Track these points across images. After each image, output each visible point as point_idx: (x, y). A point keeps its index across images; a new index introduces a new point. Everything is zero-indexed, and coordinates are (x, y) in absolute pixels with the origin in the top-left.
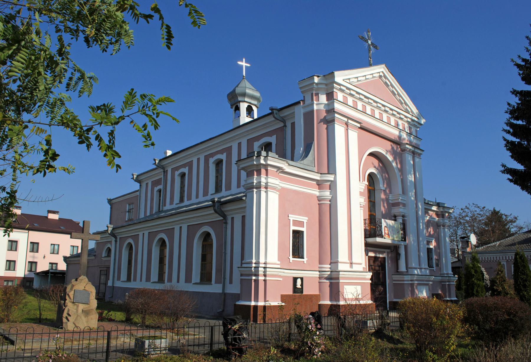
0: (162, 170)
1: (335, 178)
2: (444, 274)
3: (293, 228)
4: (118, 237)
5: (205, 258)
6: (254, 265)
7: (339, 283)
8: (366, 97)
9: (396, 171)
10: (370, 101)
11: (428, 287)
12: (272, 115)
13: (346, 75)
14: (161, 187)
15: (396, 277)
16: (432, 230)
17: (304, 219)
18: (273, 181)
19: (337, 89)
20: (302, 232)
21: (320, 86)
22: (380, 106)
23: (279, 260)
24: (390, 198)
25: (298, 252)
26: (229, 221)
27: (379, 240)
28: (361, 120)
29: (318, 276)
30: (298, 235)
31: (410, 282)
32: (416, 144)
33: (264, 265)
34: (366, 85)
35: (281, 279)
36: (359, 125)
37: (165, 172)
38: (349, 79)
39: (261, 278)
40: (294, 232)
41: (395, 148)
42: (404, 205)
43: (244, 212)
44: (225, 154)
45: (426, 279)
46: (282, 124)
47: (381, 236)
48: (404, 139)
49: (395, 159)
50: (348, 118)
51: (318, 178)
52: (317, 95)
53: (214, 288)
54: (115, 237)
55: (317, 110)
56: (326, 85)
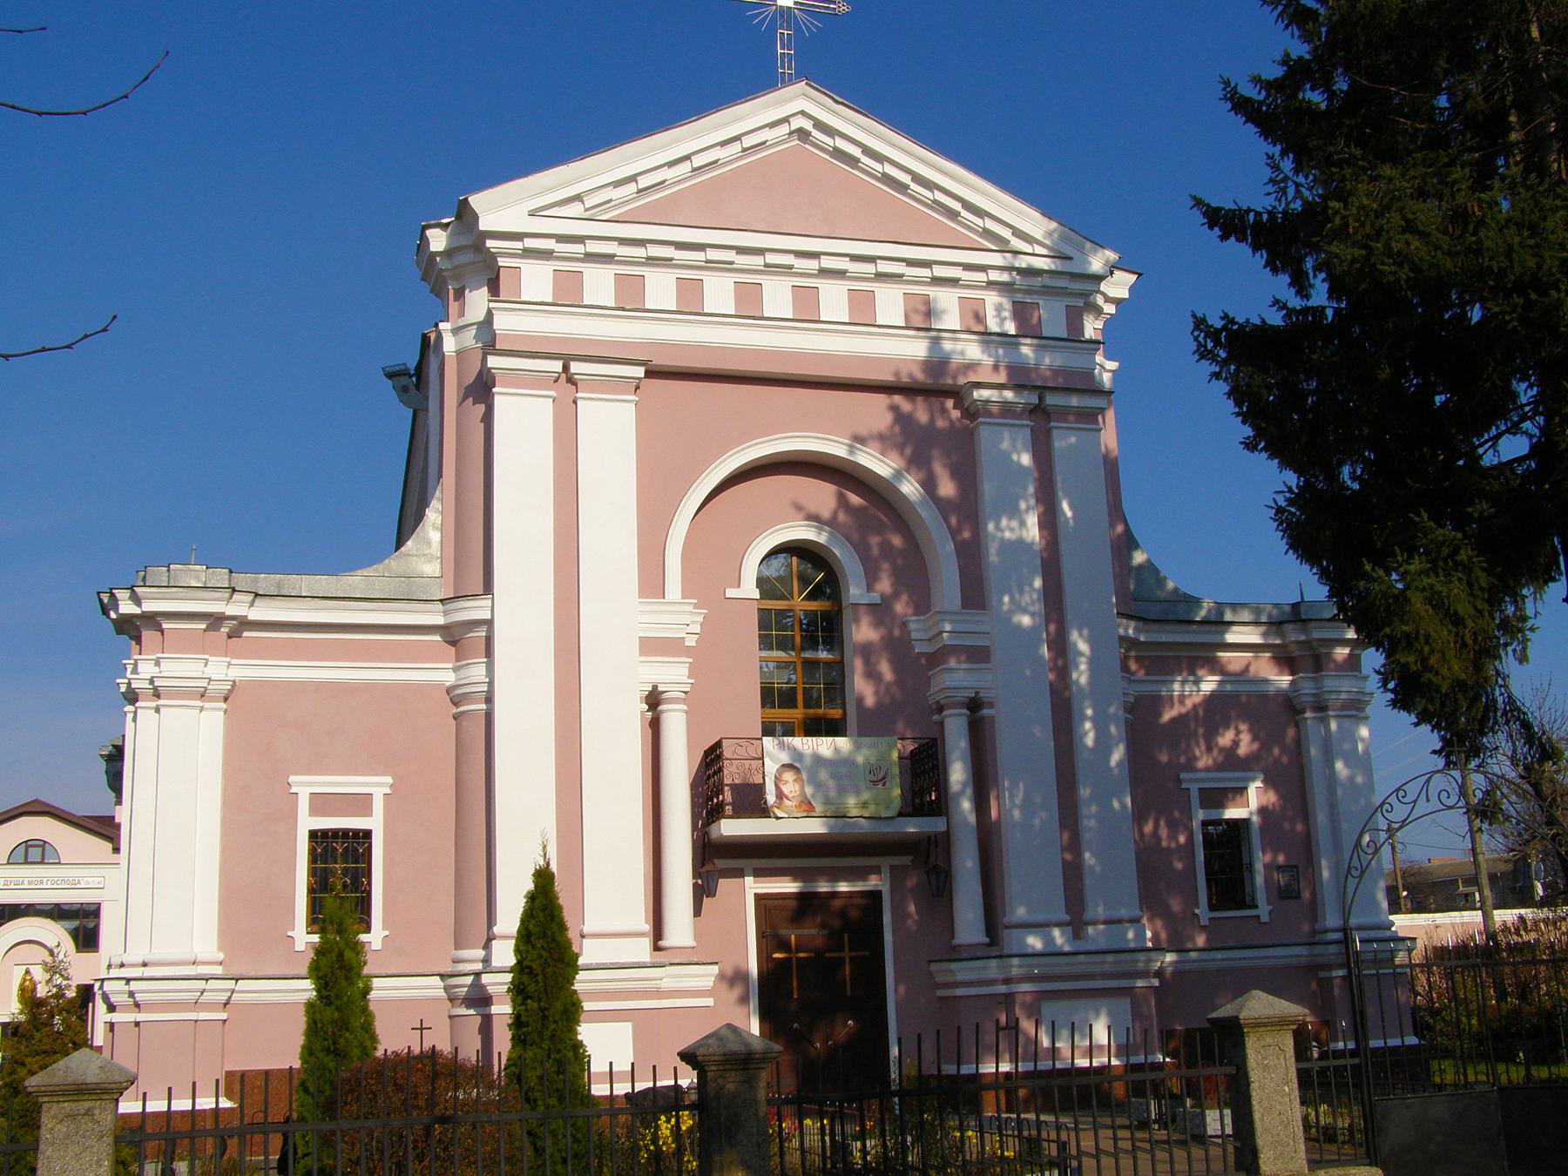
2: (1326, 931)
3: (308, 822)
9: (928, 515)
11: (1124, 1004)
16: (1245, 738)
20: (368, 834)
21: (460, 260)
23: (220, 948)
24: (914, 635)
28: (427, 383)
31: (1002, 989)
32: (1057, 372)
34: (711, 196)
41: (922, 416)
42: (979, 655)
45: (1107, 968)
47: (763, 812)
48: (972, 366)
49: (918, 462)
50: (567, 360)
51: (440, 620)
52: (460, 294)
55: (458, 353)
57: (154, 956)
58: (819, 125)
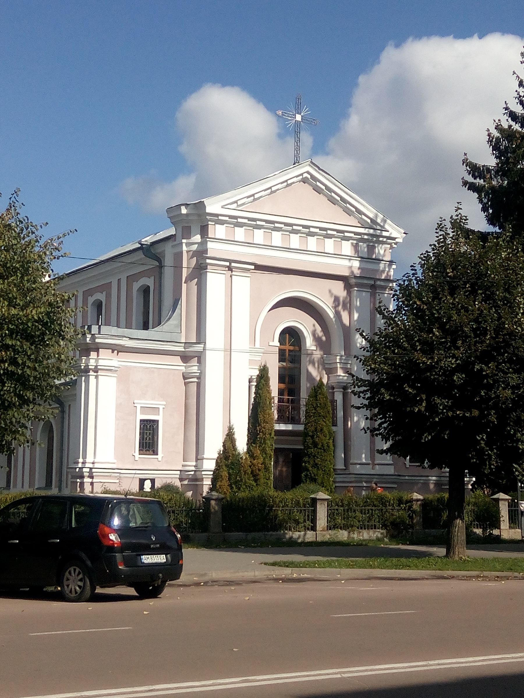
1: (204, 349)
6: (80, 465)
7: (203, 485)
17: (160, 404)
20: (158, 421)
26: (67, 409)
29: (178, 476)
33: (91, 466)
36: (253, 267)
39: (87, 480)
44: (104, 293)
50: (230, 261)
58: (312, 177)
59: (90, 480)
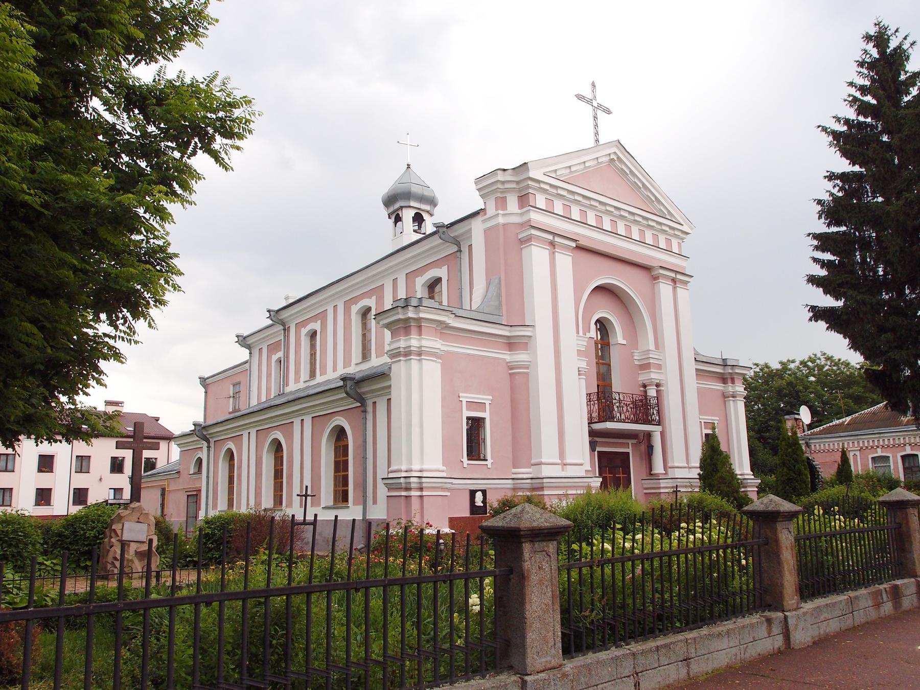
0: (282, 327)
3: (467, 413)
4: (212, 441)
5: (341, 466)
8: (584, 197)
10: (593, 203)
12: (436, 236)
13: (549, 165)
14: (280, 354)
15: (648, 483)
17: (486, 399)
18: (430, 342)
19: (534, 189)
20: (484, 419)
22: (612, 209)
25: (475, 449)
26: (370, 409)
27: (609, 425)
30: (475, 426)
35: (448, 494)
37: (286, 330)
38: (555, 171)
40: (468, 418)
42: (659, 367)
43: (390, 393)
44: (374, 298)
46: (455, 248)
53: (351, 513)
54: (208, 441)
56: (518, 183)
57: (425, 467)
58: (618, 158)
59: (419, 493)
